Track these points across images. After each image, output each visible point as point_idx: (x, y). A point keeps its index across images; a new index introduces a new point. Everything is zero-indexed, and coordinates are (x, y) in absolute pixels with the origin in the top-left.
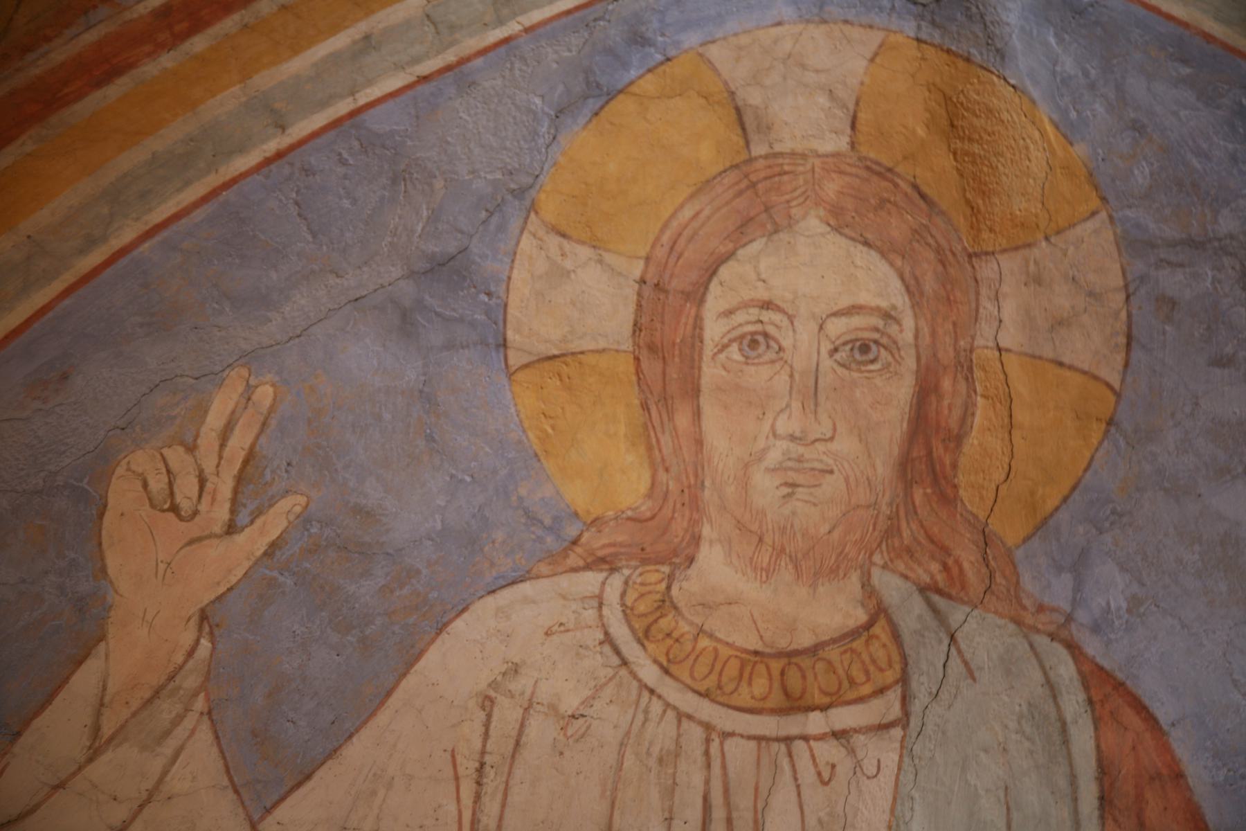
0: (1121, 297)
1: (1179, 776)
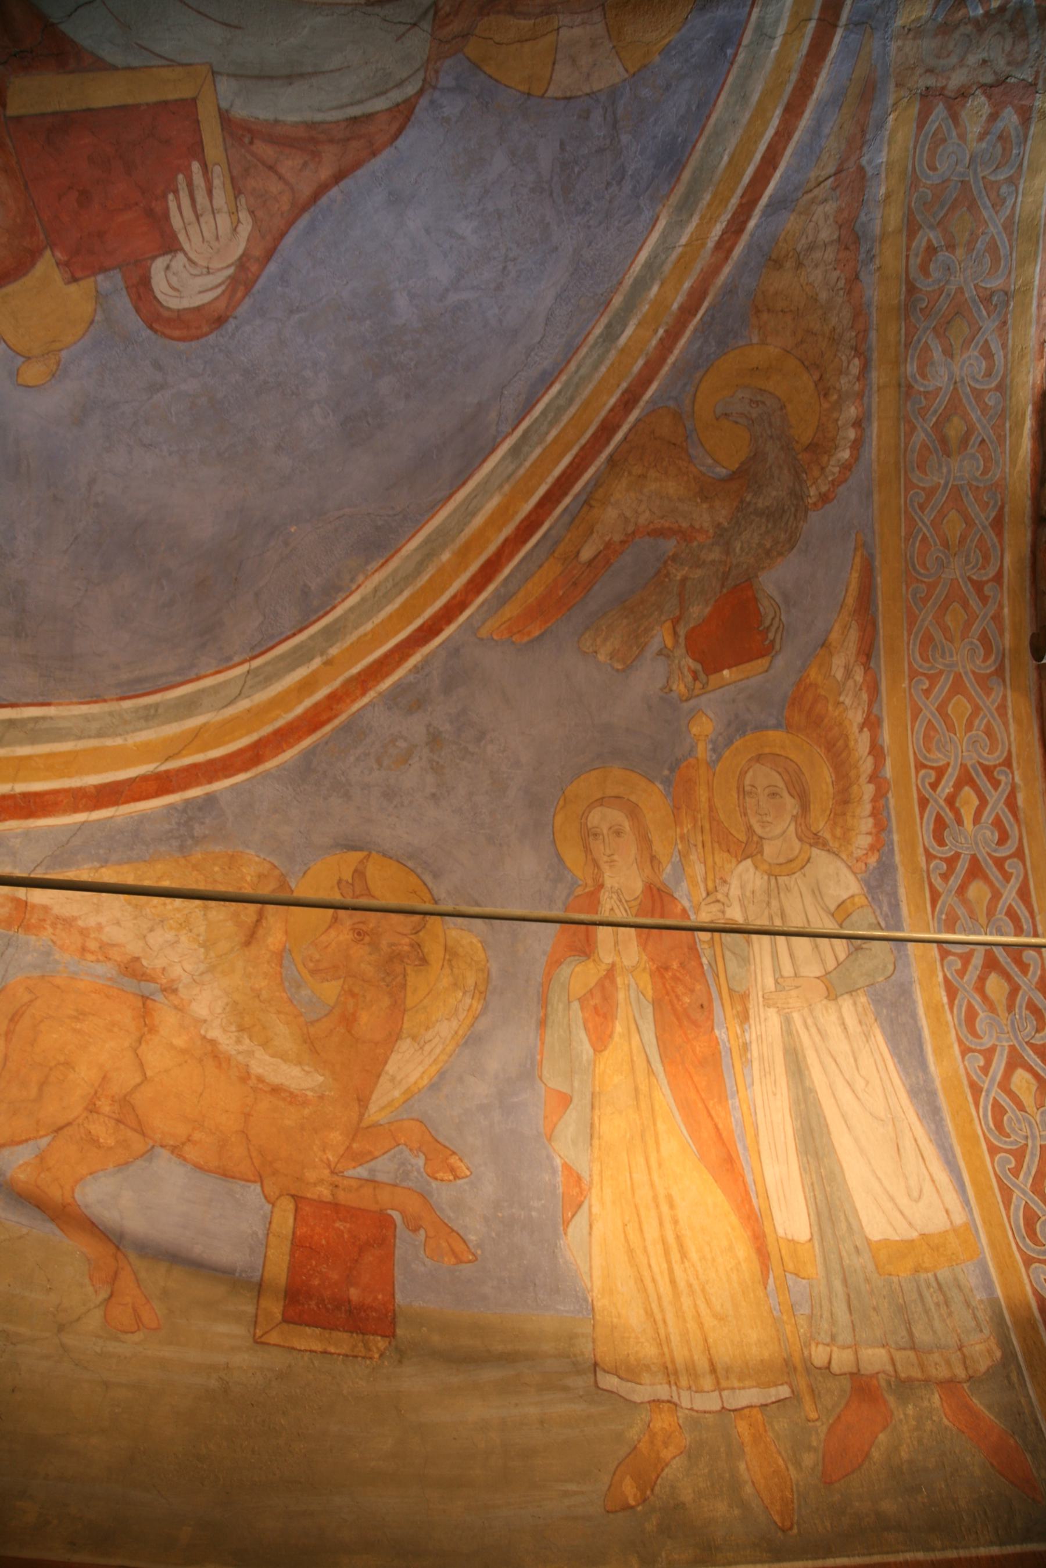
0: (588, 90)
1: (374, 154)
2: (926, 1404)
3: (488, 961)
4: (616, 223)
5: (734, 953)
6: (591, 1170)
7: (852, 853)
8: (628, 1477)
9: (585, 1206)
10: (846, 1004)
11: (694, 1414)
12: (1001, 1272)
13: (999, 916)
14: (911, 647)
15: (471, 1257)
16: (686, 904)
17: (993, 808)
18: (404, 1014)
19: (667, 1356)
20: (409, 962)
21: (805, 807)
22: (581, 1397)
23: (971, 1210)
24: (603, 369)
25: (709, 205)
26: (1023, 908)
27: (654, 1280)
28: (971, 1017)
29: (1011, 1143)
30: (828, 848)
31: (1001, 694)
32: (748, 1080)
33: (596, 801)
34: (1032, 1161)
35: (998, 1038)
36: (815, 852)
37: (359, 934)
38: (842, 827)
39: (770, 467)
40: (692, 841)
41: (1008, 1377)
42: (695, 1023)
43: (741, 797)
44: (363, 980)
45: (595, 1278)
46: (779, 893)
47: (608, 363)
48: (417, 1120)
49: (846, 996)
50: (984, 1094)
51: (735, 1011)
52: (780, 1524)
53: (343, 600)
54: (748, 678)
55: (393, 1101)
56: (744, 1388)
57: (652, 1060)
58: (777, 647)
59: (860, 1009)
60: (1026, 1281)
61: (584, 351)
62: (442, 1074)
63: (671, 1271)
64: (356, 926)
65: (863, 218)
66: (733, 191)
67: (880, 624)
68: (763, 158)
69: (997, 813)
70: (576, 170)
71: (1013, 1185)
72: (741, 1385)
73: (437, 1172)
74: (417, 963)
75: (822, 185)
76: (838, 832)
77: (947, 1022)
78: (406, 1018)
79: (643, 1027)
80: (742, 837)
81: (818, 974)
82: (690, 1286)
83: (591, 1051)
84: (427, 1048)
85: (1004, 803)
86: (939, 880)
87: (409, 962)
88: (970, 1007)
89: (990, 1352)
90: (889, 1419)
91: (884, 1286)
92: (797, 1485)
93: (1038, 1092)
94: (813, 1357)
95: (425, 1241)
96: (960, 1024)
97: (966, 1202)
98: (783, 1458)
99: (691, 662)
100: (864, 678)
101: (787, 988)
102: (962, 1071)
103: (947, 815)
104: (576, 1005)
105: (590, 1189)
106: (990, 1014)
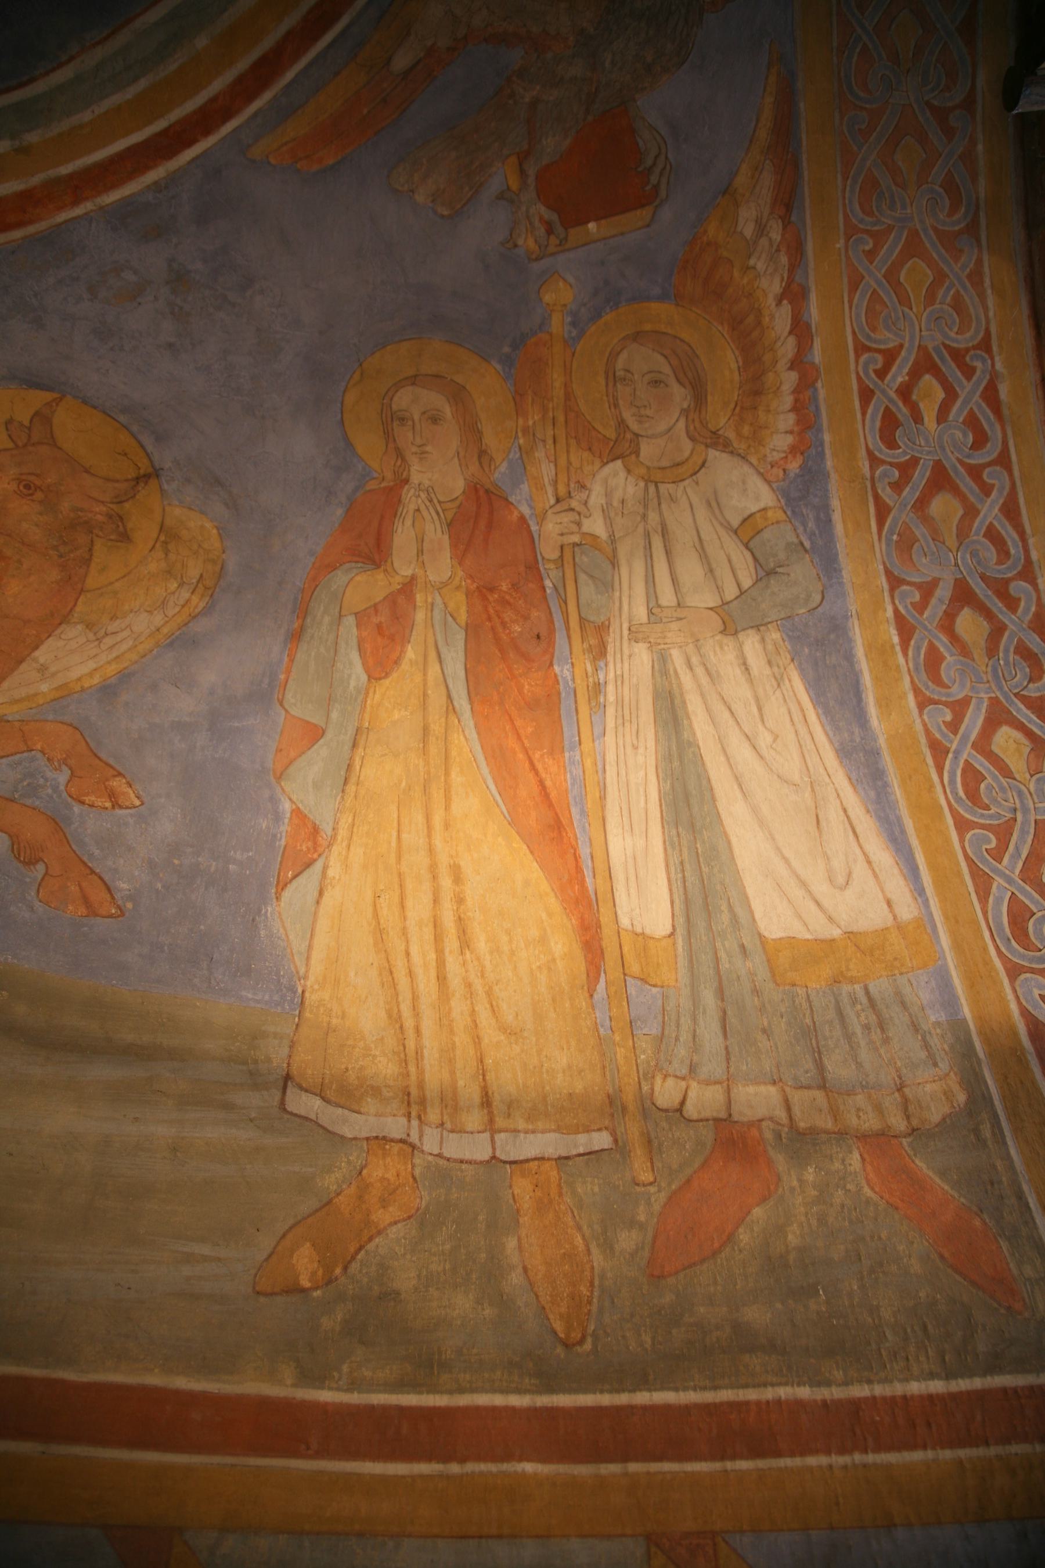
2: (837, 1165)
3: (224, 552)
5: (592, 577)
6: (336, 822)
7: (765, 456)
8: (308, 1244)
9: (318, 865)
10: (751, 643)
11: (441, 1162)
12: (971, 984)
13: (975, 538)
14: (847, 195)
15: (113, 911)
16: (526, 510)
17: (966, 402)
18: (80, 594)
19: (413, 1078)
20: (101, 534)
21: (699, 397)
22: (251, 1120)
23: (926, 903)
26: (1010, 528)
27: (411, 974)
28: (933, 662)
29: (991, 817)
30: (731, 448)
31: (974, 258)
32: (597, 731)
33: (406, 378)
34: (1022, 838)
35: (972, 688)
36: (712, 453)
37: (27, 487)
38: (751, 424)
40: (539, 435)
41: (976, 1132)
42: (525, 656)
43: (611, 384)
44: (23, 543)
45: (313, 962)
46: (659, 504)
48: (71, 725)
49: (750, 632)
50: (950, 755)
51: (586, 645)
52: (562, 1335)
53: (47, 73)
54: (622, 234)
55: (36, 695)
56: (533, 1132)
57: (454, 694)
58: (663, 193)
59: (770, 647)
60: (1010, 996)
62: (125, 677)
63: (441, 963)
64: (24, 477)
67: (805, 164)
69: (971, 409)
71: (992, 871)
72: (530, 1127)
73: (87, 794)
74: (113, 537)
76: (746, 430)
77: (898, 667)
78: (82, 599)
79: (448, 655)
80: (611, 434)
81: (711, 605)
82: (469, 985)
83: (364, 677)
84: (108, 641)
85: (981, 396)
86: (888, 490)
87: (101, 534)
88: (932, 649)
89: (948, 1095)
90: (772, 1187)
91: (783, 1000)
92: (603, 1277)
93: (1032, 755)
94: (656, 1093)
95: (43, 879)
96: (917, 669)
97: (919, 891)
98: (583, 1236)
99: (543, 210)
100: (783, 235)
101: (664, 620)
102: (919, 727)
103: (900, 410)
104: (350, 621)
105: (330, 845)
106: (961, 658)
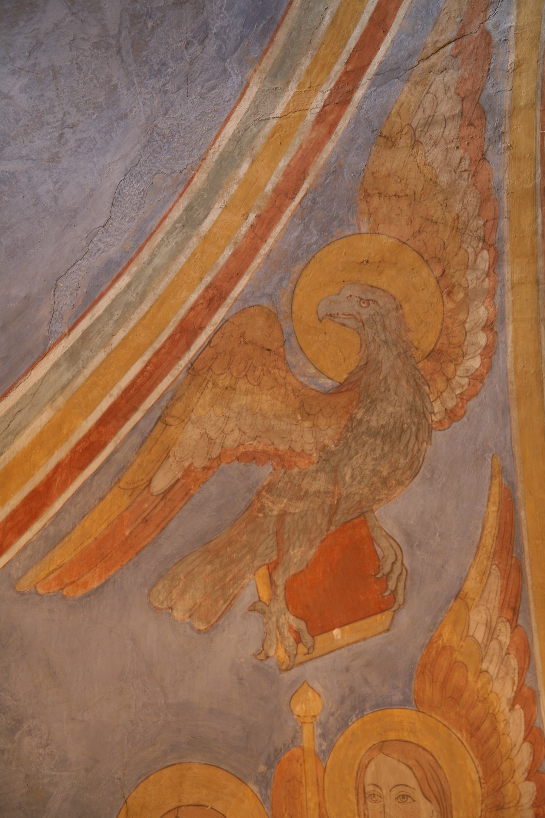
4: (198, 89)
24: (182, 259)
25: (309, 72)
39: (385, 378)
43: (361, 802)
47: (188, 252)
54: (364, 639)
58: (400, 598)
61: (158, 237)
65: (489, 90)
66: (337, 56)
67: (528, 569)
68: (371, 19)
70: (150, 24)
75: (441, 51)
99: (291, 618)
100: (511, 638)
